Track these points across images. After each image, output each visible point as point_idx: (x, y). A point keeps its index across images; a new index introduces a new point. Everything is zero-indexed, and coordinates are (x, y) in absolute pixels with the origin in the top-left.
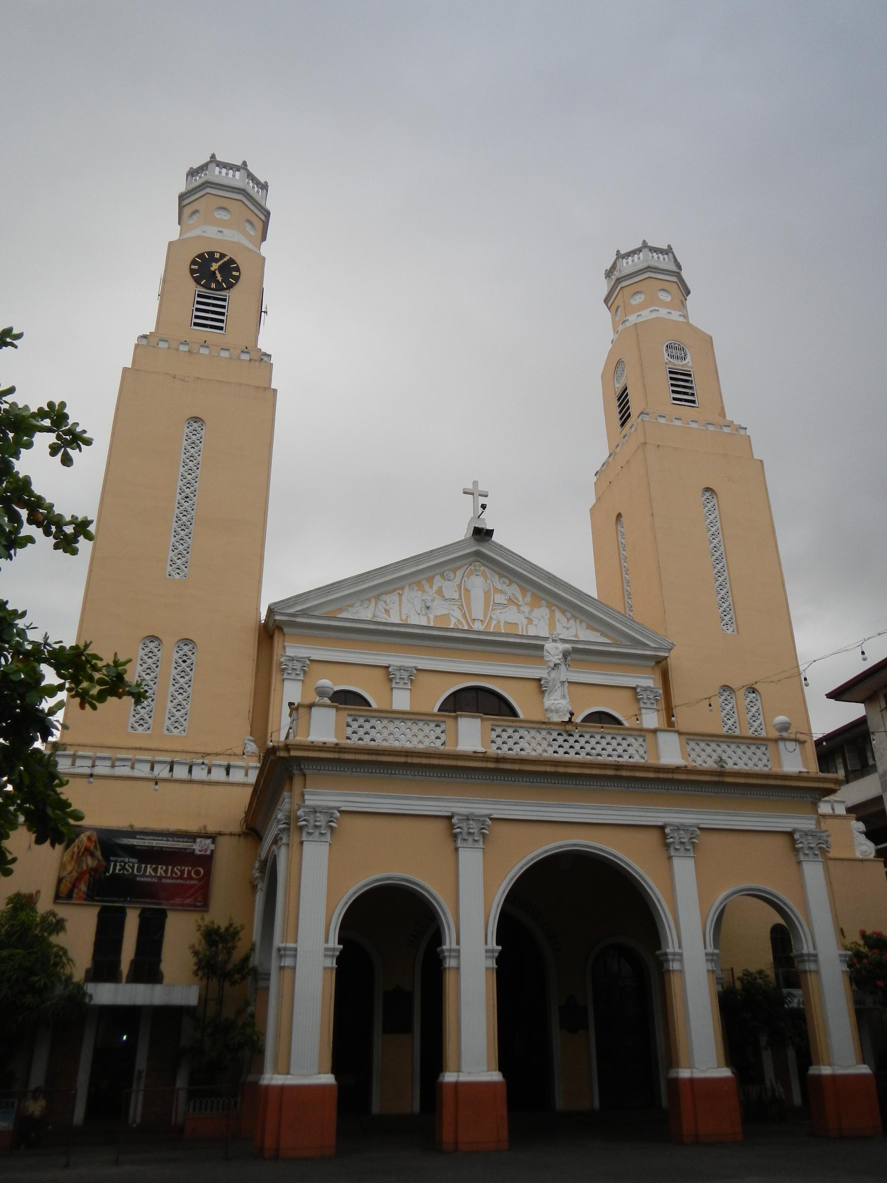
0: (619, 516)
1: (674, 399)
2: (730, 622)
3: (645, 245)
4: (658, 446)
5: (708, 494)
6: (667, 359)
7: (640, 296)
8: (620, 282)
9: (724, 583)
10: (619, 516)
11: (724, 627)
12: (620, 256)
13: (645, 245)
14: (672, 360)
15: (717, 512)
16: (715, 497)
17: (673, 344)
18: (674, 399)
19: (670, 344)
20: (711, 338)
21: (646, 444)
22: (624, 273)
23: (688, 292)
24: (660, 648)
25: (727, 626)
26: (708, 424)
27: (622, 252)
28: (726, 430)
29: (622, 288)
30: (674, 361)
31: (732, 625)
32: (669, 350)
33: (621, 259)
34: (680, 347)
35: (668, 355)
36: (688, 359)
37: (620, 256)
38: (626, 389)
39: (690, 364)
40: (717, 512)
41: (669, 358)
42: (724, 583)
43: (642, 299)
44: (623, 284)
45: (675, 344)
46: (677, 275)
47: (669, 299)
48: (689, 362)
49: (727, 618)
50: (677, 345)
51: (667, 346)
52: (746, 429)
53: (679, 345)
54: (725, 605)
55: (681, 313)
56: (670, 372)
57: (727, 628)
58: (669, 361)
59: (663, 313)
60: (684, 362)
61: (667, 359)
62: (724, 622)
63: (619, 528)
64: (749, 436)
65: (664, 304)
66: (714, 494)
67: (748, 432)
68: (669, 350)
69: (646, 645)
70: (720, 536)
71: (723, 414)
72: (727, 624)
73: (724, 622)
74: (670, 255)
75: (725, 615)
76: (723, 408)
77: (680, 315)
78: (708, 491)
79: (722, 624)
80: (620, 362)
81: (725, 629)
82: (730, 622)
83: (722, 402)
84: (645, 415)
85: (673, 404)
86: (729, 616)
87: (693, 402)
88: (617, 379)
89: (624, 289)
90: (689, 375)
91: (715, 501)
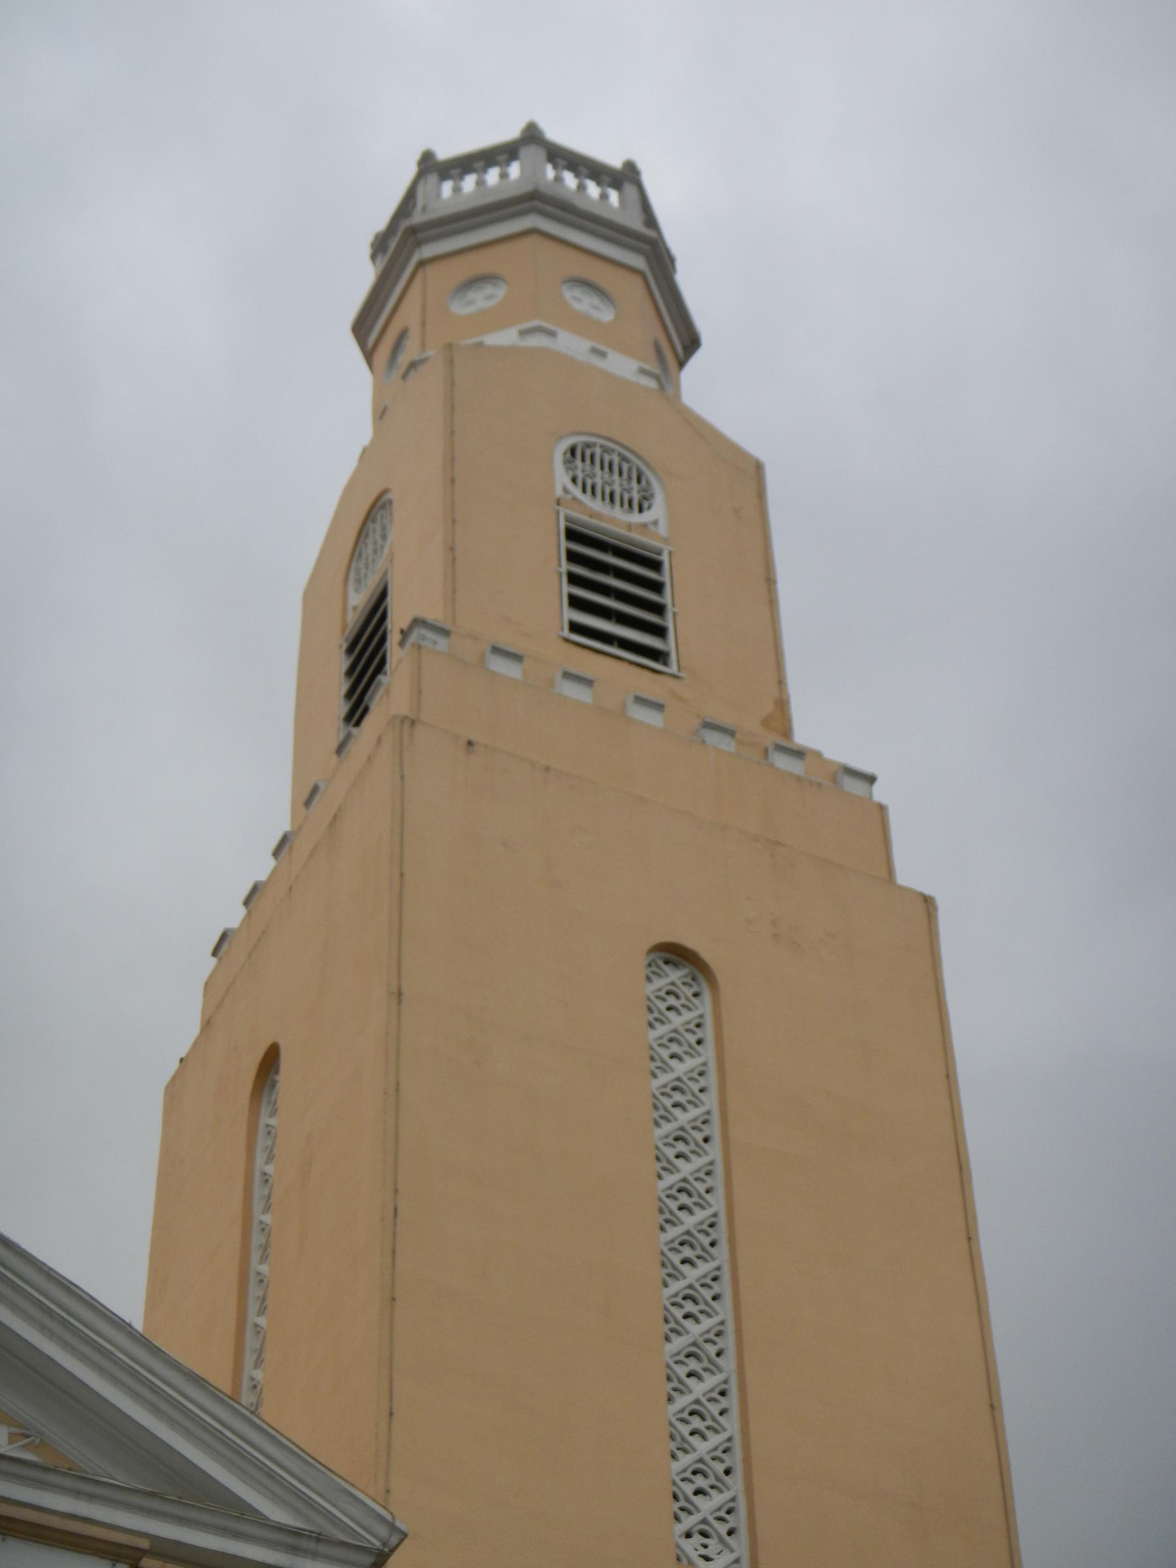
0: (271, 1060)
1: (575, 627)
2: (723, 1529)
3: (532, 135)
4: (470, 743)
5: (674, 975)
6: (566, 490)
7: (489, 290)
8: (419, 244)
9: (712, 1350)
10: (271, 1060)
11: (687, 1545)
12: (429, 165)
13: (532, 135)
14: (586, 499)
15: (708, 1052)
16: (707, 996)
17: (598, 451)
18: (575, 627)
19: (588, 445)
20: (759, 468)
21: (413, 723)
22: (437, 212)
23: (692, 343)
24: (319, 1538)
25: (705, 1541)
26: (709, 726)
27: (445, 152)
28: (782, 762)
29: (422, 263)
30: (597, 505)
31: (728, 1539)
32: (578, 462)
33: (433, 179)
34: (625, 466)
35: (574, 480)
36: (657, 511)
37: (429, 165)
38: (383, 595)
39: (662, 530)
40: (708, 1052)
41: (577, 491)
42: (712, 1350)
43: (490, 304)
44: (428, 251)
45: (606, 450)
46: (647, 247)
47: (606, 315)
48: (655, 523)
49: (706, 1506)
50: (616, 459)
51: (573, 451)
52: (871, 779)
53: (624, 459)
54: (702, 1447)
55: (647, 367)
56: (572, 535)
57: (703, 1551)
58: (575, 499)
59: (572, 344)
60: (636, 518)
61: (566, 490)
62: (688, 1522)
63: (264, 1120)
64: (882, 809)
65: (582, 325)
66: (702, 979)
67: (879, 793)
68: (578, 462)
69: (243, 1511)
70: (714, 1151)
71: (787, 732)
72: (704, 1534)
73: (688, 1522)
74: (630, 189)
75: (697, 1492)
76: (782, 705)
77: (643, 372)
78: (676, 965)
79: (680, 1528)
80: (379, 507)
81: (694, 1556)
82: (723, 1529)
83: (781, 682)
84: (429, 634)
85: (567, 640)
86: (717, 1499)
87: (658, 655)
88: (358, 581)
89: (431, 271)
90: (656, 566)
91: (705, 1006)
